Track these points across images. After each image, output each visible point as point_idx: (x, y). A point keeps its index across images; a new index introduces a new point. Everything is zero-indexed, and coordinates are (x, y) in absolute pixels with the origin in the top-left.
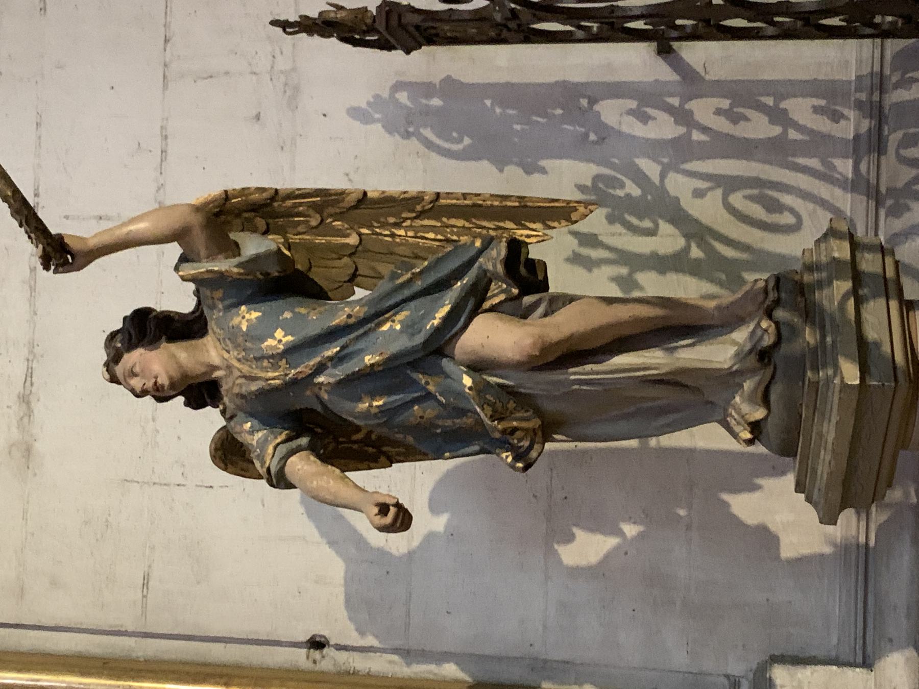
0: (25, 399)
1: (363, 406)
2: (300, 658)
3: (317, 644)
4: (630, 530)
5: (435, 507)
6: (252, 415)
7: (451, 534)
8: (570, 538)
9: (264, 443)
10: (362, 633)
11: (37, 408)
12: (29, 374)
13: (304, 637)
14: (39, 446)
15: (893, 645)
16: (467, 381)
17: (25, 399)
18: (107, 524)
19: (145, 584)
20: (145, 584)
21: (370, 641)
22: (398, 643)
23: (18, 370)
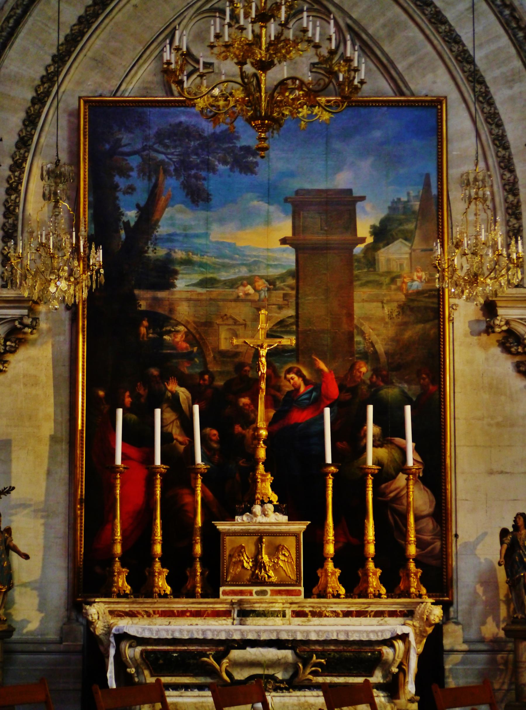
0: (502, 472)
1: (517, 558)
2: (454, 533)
3: (456, 536)
4: (484, 598)
5: (486, 559)
6: (513, 537)
7: (480, 563)
8: (481, 586)
9: (508, 540)
10: (460, 545)
11: (501, 475)
12: (507, 473)
13: (458, 533)
14: (493, 476)
15: (469, 646)
16: (522, 574)
17: (502, 472)
18: (478, 491)
19: (467, 500)
20: (467, 500)
21: (458, 547)
22: (458, 553)
23: (508, 471)
